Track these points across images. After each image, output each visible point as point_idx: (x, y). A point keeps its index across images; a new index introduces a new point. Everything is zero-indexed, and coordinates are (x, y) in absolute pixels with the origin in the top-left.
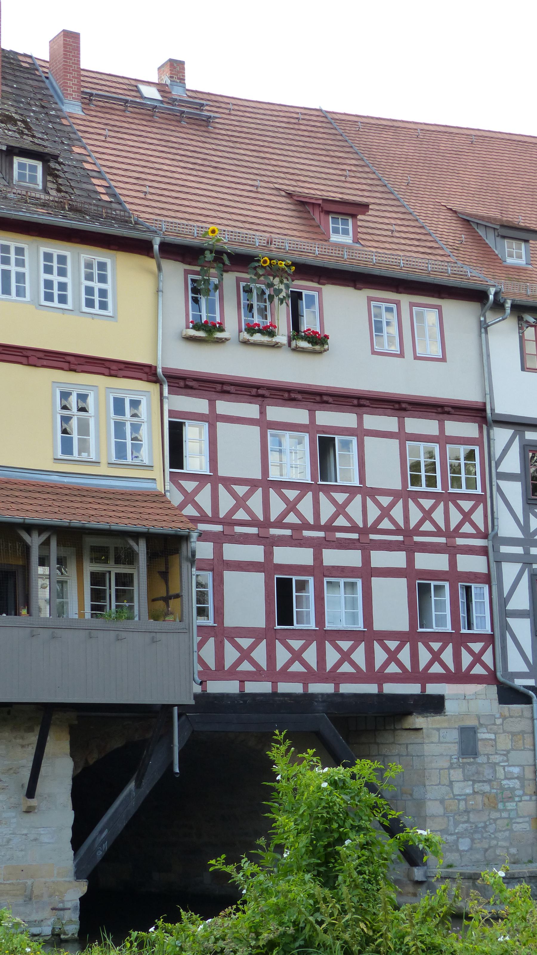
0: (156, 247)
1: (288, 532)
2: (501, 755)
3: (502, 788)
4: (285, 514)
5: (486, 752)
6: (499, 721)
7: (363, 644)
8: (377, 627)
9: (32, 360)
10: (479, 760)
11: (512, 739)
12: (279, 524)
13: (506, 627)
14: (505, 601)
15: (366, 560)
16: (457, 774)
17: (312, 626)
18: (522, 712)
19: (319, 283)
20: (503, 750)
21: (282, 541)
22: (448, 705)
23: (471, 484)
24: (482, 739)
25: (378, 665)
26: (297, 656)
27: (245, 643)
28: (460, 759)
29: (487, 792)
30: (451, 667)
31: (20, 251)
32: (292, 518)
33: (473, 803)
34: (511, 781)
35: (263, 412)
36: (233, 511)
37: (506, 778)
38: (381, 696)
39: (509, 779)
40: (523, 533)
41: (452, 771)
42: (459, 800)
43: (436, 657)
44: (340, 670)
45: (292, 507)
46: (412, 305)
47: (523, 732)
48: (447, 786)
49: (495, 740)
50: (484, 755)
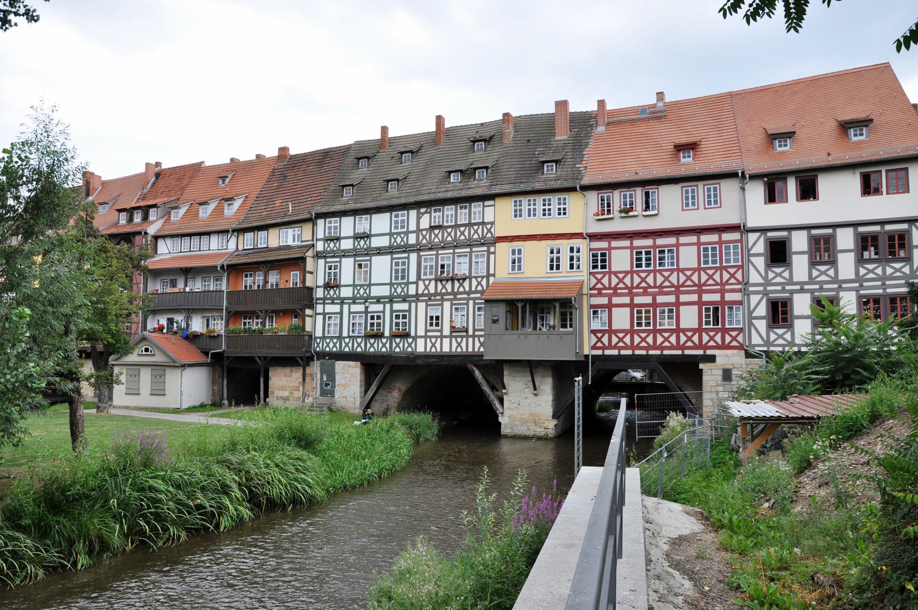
0: (578, 189)
1: (642, 290)
4: (640, 283)
7: (675, 334)
8: (682, 326)
9: (539, 238)
10: (732, 383)
12: (638, 287)
13: (751, 324)
15: (678, 298)
16: (721, 389)
17: (651, 327)
21: (637, 294)
22: (717, 359)
23: (736, 260)
25: (682, 342)
26: (643, 340)
27: (621, 335)
30: (720, 343)
31: (535, 200)
32: (643, 285)
35: (632, 243)
36: (618, 284)
38: (683, 355)
40: (764, 280)
43: (712, 338)
44: (663, 345)
45: (643, 280)
46: (704, 185)
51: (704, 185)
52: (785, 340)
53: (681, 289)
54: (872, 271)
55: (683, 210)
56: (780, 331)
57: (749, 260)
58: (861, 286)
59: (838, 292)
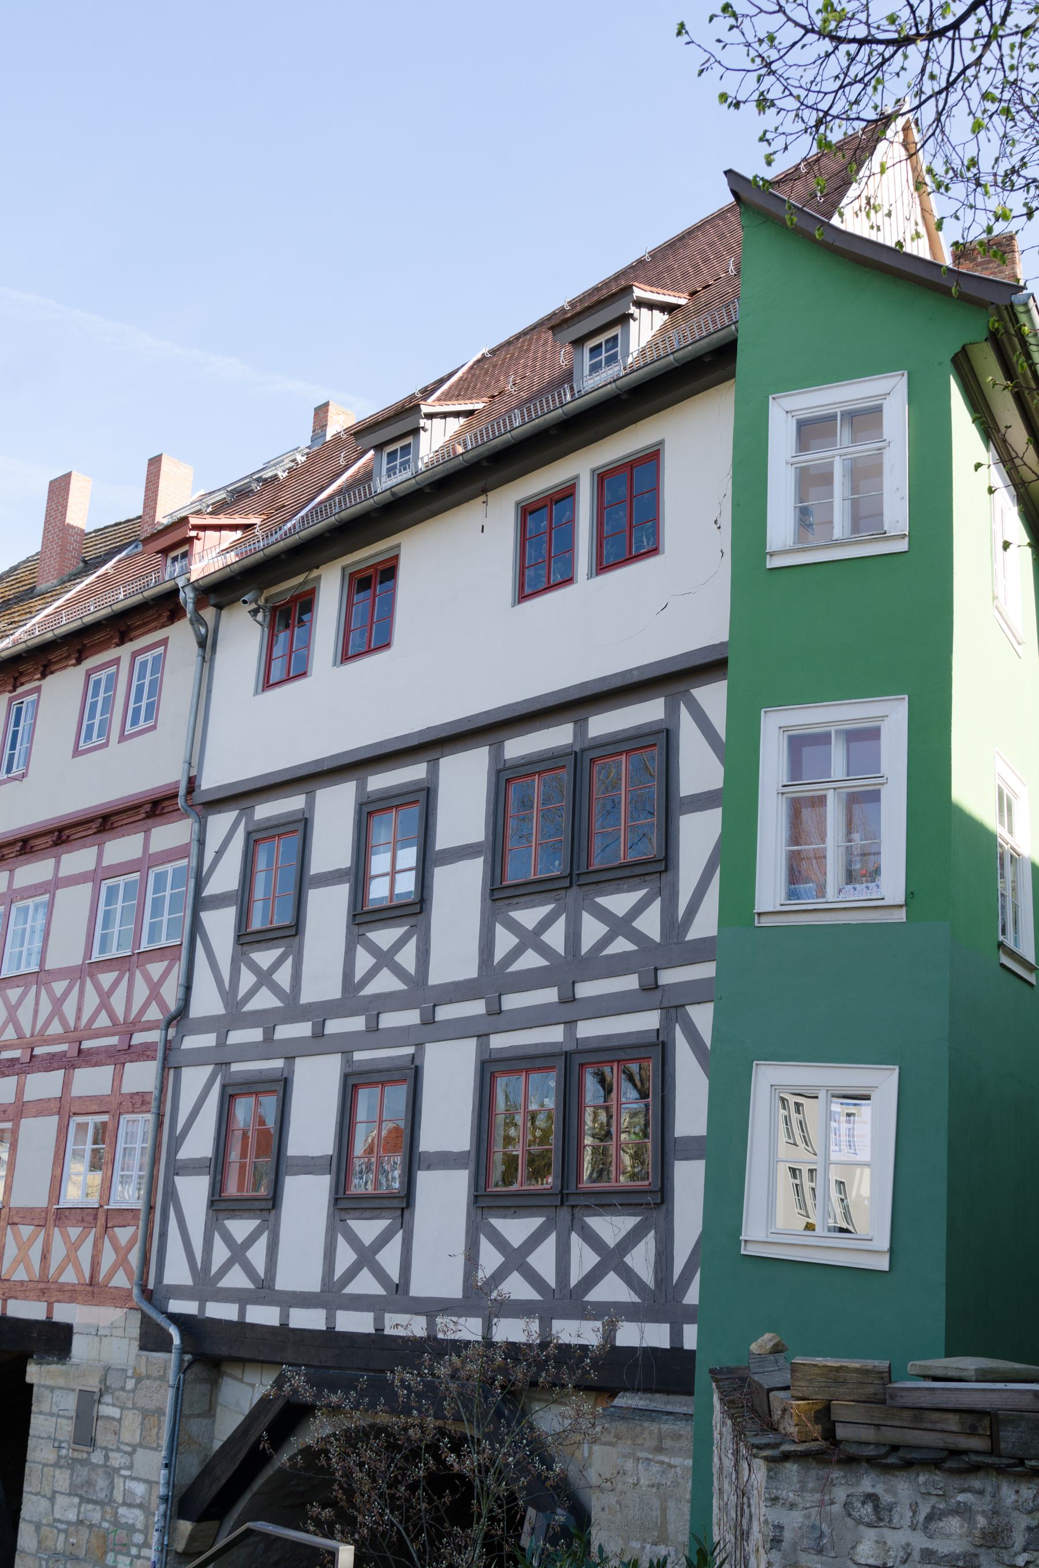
2: (125, 1453)
3: (116, 1523)
5: (105, 1444)
6: (130, 1384)
10: (97, 1457)
11: (142, 1424)
13: (171, 1194)
14: (177, 1142)
16: (62, 1479)
18: (165, 1370)
19: (39, 679)
20: (127, 1444)
24: (103, 1417)
28: (71, 1451)
29: (95, 1525)
33: (75, 1541)
34: (132, 1510)
37: (125, 1504)
39: (130, 1506)
41: (58, 1472)
42: (59, 1531)
47: (160, 1412)
48: (48, 1499)
49: (119, 1420)
50: (103, 1448)
51: (135, 655)
52: (249, 1270)
53: (38, 1051)
54: (530, 939)
55: (77, 752)
56: (240, 1228)
57: (196, 927)
58: (495, 1011)
59: (420, 1046)
